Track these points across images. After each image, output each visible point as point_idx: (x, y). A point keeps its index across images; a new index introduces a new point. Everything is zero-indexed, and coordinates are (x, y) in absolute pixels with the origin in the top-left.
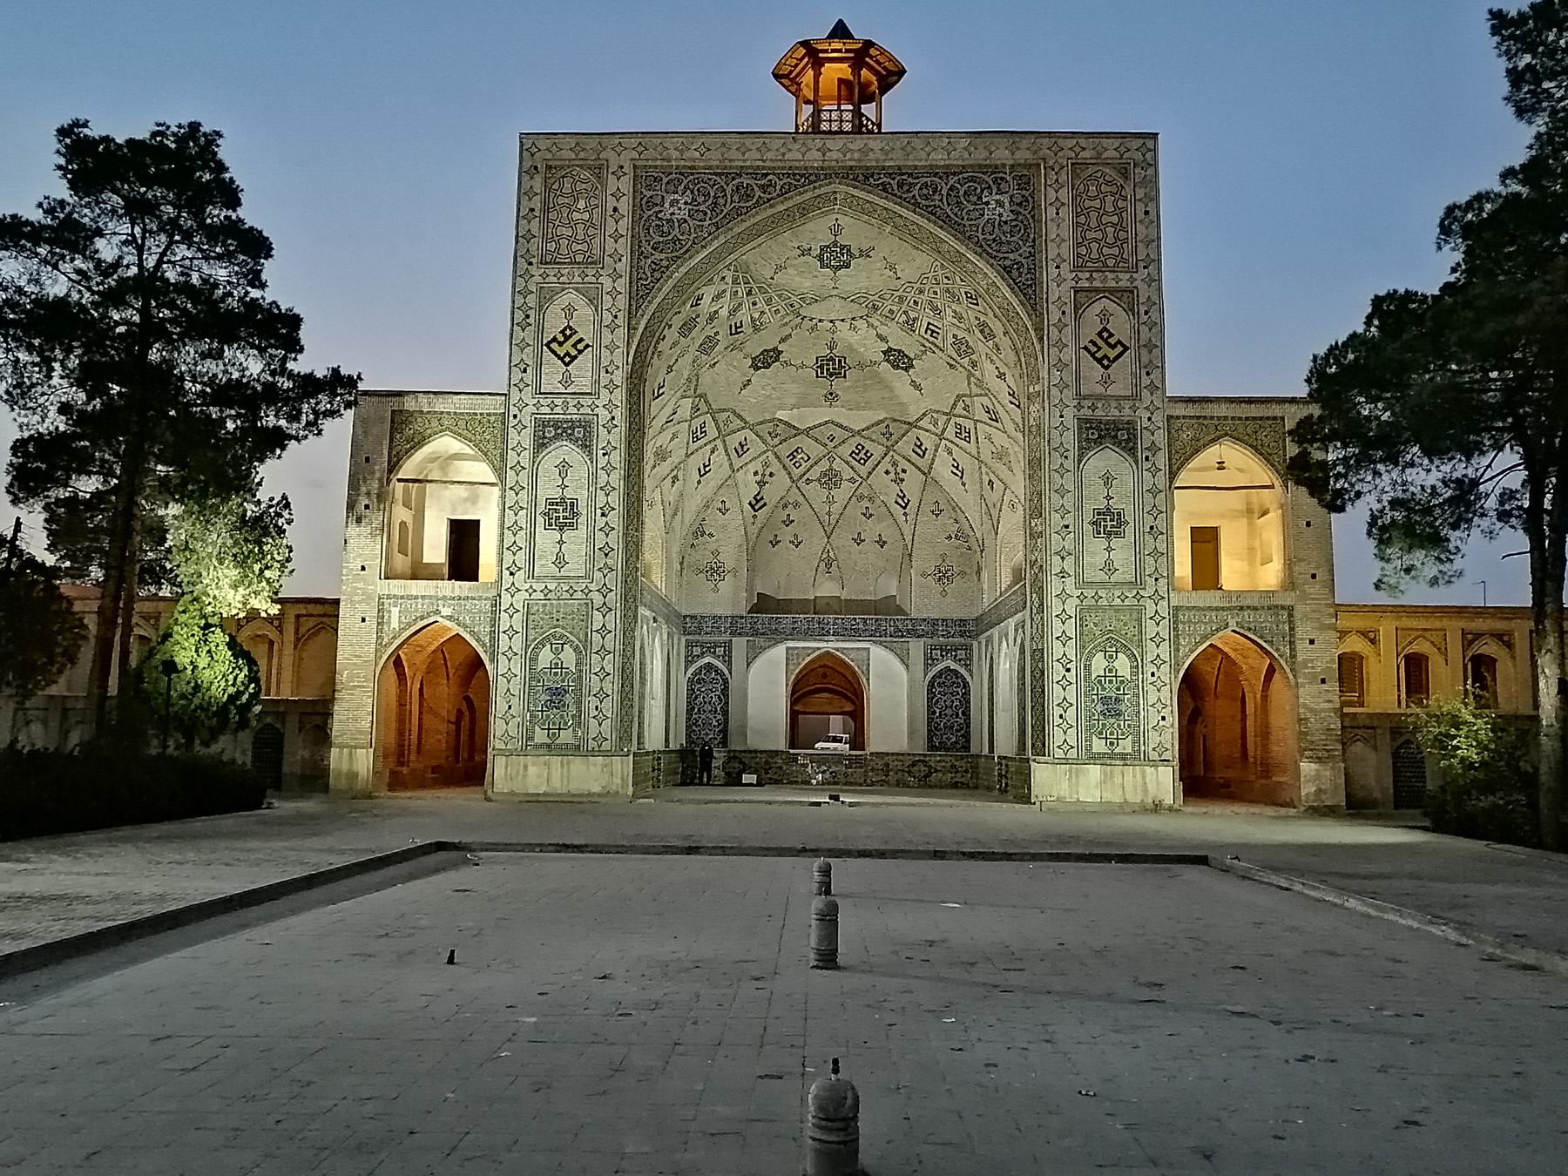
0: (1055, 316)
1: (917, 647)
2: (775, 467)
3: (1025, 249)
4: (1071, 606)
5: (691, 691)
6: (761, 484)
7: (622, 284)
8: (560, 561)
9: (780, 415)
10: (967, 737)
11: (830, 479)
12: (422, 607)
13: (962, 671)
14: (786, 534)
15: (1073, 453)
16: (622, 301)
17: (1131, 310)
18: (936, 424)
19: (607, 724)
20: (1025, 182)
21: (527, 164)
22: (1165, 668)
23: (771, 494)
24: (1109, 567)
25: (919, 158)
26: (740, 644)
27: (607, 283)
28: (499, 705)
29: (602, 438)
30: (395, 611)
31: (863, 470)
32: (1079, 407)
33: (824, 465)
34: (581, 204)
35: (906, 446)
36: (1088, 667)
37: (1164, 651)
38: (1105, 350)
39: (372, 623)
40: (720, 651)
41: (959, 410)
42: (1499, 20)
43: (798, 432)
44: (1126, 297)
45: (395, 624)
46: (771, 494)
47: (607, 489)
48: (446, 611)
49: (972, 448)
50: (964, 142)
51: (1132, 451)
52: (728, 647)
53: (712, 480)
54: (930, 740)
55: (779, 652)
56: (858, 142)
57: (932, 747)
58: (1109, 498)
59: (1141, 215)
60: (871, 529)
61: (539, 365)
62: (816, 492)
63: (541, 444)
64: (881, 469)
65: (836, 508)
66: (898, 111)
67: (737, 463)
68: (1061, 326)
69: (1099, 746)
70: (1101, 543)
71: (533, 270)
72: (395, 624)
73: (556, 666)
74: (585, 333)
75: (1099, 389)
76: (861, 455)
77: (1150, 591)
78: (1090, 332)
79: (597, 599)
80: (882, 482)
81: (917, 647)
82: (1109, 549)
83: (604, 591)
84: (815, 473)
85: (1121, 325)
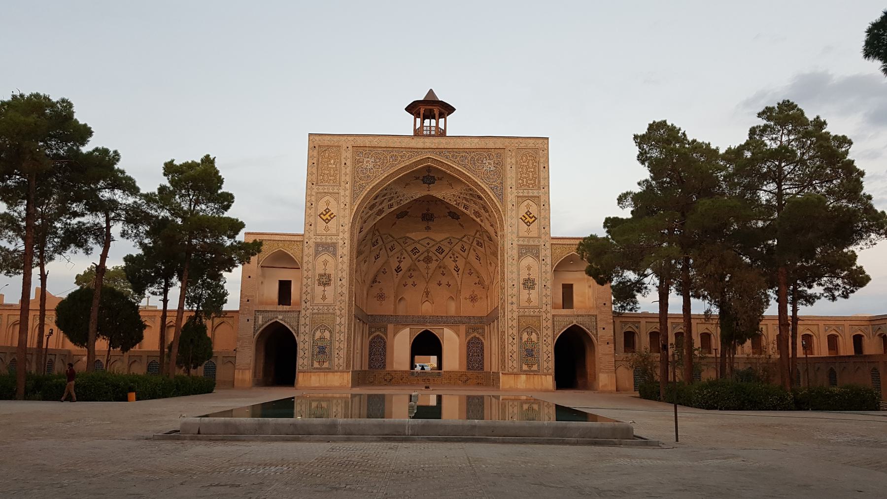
0: (510, 206)
1: (463, 328)
2: (405, 255)
3: (499, 181)
4: (515, 315)
5: (371, 345)
6: (400, 262)
7: (348, 193)
8: (324, 298)
9: (407, 235)
10: (482, 364)
11: (428, 260)
12: (271, 315)
13: (481, 338)
14: (410, 281)
15: (516, 257)
16: (348, 200)
17: (538, 205)
18: (469, 239)
19: (341, 361)
20: (499, 156)
21: (312, 146)
22: (550, 339)
23: (404, 266)
24: (529, 300)
25: (461, 144)
26: (390, 327)
27: (342, 193)
28: (300, 353)
29: (340, 252)
30: (260, 317)
31: (441, 256)
32: (518, 241)
33: (426, 254)
34: (332, 161)
35: (458, 248)
36: (521, 338)
37: (550, 332)
38: (529, 219)
39: (252, 322)
40: (383, 330)
41: (478, 235)
42: (636, 137)
43: (415, 242)
44: (536, 199)
45: (260, 322)
46: (404, 266)
47: (342, 270)
48: (280, 317)
49: (482, 250)
50: (477, 140)
51: (538, 257)
52: (386, 329)
53: (381, 261)
54: (468, 366)
55: (407, 330)
56: (437, 140)
57: (468, 369)
58: (529, 274)
59: (542, 168)
60: (444, 280)
61: (316, 223)
62: (422, 265)
63: (317, 253)
64: (448, 256)
65: (431, 271)
66: (454, 126)
67: (391, 254)
68: (512, 210)
69: (525, 367)
70: (527, 291)
71: (314, 186)
72: (260, 322)
73: (322, 339)
74: (333, 211)
75: (526, 234)
76: (440, 250)
77: (544, 309)
78: (523, 211)
79: (338, 312)
80: (450, 263)
81: (463, 328)
82: (529, 294)
83: (341, 309)
84: (422, 258)
85: (534, 210)
